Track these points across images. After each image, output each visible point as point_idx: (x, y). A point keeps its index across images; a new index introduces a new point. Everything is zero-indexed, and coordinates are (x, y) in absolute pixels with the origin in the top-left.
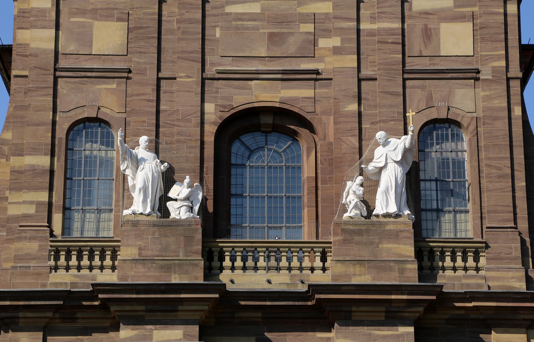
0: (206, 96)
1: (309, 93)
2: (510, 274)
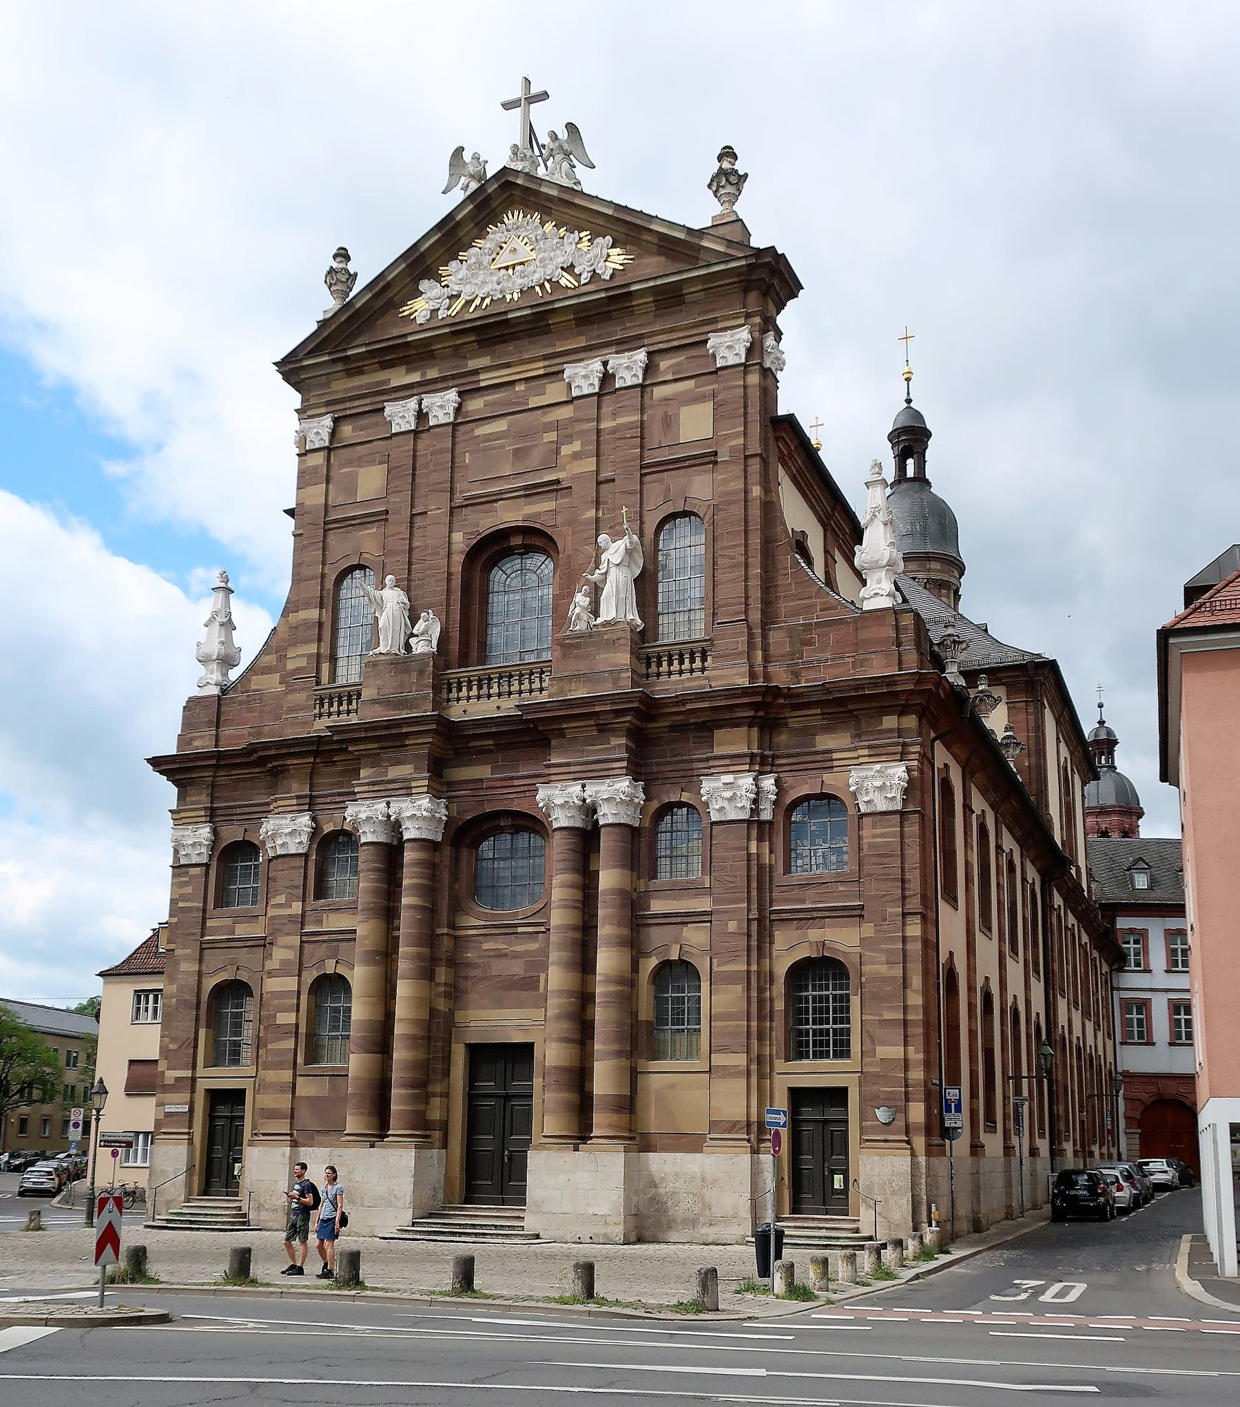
0: (455, 526)
2: (734, 671)
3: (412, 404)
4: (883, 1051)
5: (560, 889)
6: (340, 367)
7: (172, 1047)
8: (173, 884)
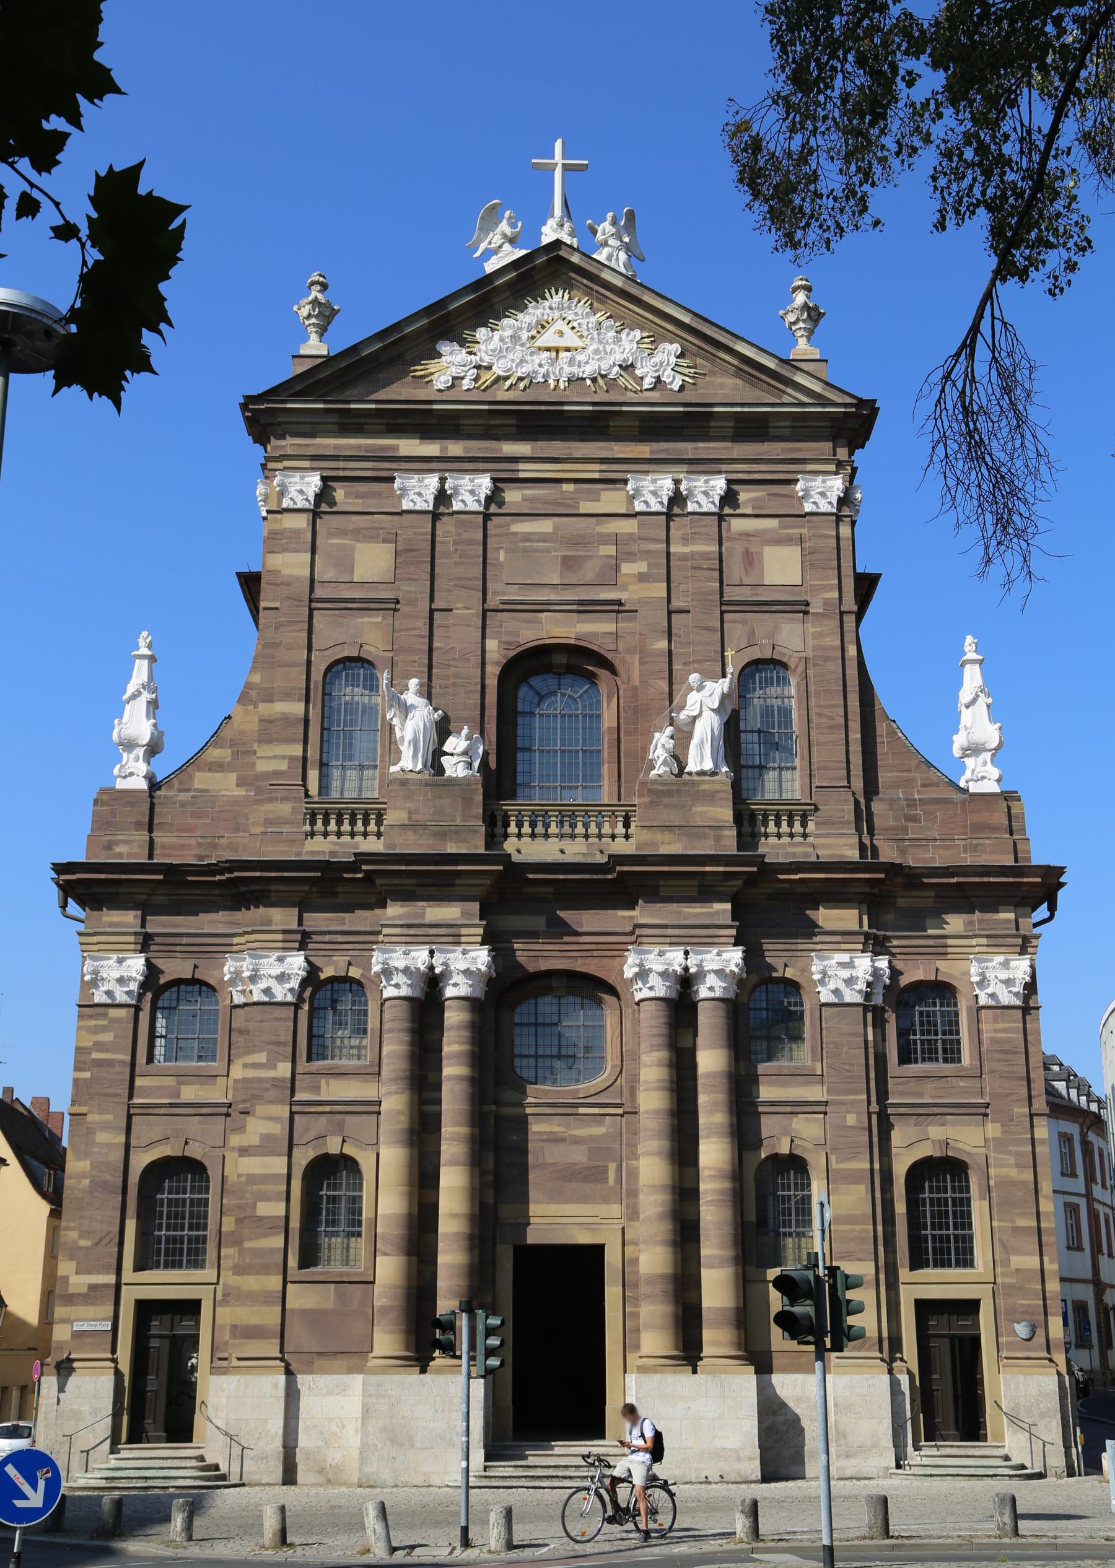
1: (611, 627)
2: (842, 841)
3: (432, 482)
5: (652, 1070)
6: (334, 419)
7: (84, 1243)
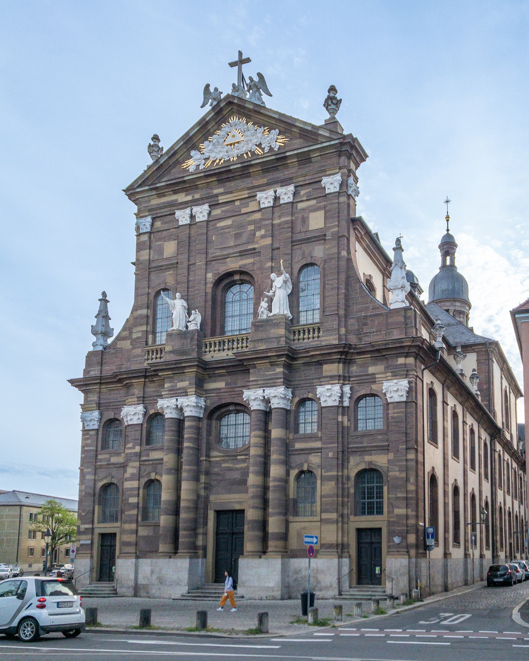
0: (208, 270)
1: (251, 260)
2: (331, 338)
4: (397, 511)
7: (83, 514)
8: (82, 439)
